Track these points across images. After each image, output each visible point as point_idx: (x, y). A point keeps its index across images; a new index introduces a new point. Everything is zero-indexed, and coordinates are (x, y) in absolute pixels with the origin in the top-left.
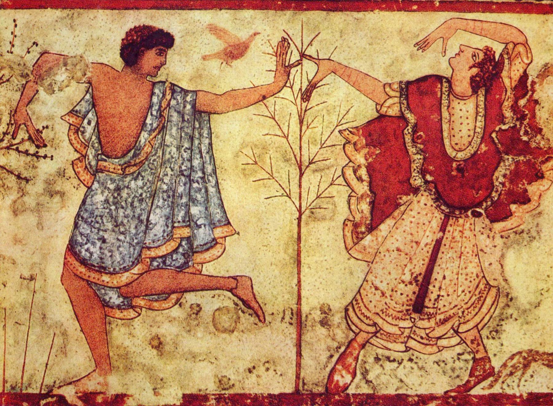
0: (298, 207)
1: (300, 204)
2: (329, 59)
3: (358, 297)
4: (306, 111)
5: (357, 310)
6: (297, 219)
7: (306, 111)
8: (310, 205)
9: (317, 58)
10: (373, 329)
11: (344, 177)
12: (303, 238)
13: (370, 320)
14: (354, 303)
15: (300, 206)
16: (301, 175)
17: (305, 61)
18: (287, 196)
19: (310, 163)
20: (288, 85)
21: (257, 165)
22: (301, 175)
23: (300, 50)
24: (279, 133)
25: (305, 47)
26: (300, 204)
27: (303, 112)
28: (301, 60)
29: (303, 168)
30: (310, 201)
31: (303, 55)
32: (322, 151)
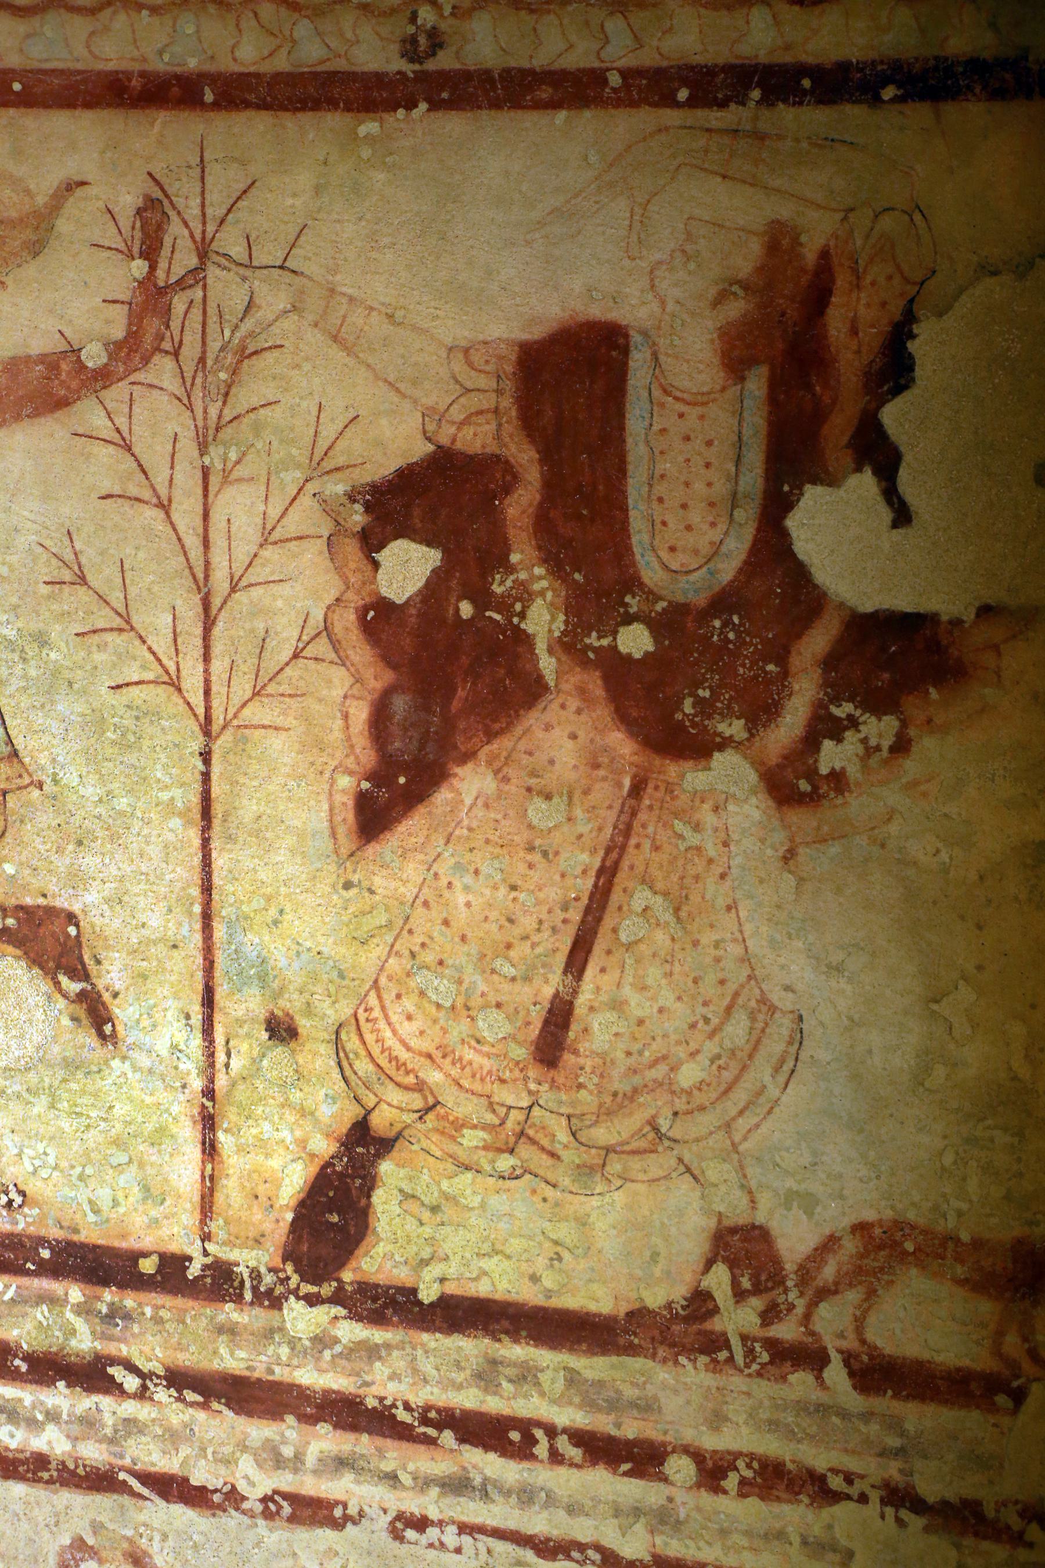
0: (202, 718)
1: (208, 709)
2: (281, 267)
3: (373, 1000)
4: (217, 429)
5: (370, 1038)
6: (201, 754)
7: (217, 429)
8: (235, 716)
9: (246, 261)
13: (408, 1073)
15: (208, 718)
16: (208, 624)
17: (213, 273)
18: (172, 684)
19: (233, 589)
20: (167, 345)
21: (82, 590)
22: (208, 624)
23: (198, 237)
24: (147, 494)
25: (211, 228)
26: (208, 709)
27: (211, 432)
29: (216, 602)
30: (236, 701)
31: (203, 252)
32: (267, 553)
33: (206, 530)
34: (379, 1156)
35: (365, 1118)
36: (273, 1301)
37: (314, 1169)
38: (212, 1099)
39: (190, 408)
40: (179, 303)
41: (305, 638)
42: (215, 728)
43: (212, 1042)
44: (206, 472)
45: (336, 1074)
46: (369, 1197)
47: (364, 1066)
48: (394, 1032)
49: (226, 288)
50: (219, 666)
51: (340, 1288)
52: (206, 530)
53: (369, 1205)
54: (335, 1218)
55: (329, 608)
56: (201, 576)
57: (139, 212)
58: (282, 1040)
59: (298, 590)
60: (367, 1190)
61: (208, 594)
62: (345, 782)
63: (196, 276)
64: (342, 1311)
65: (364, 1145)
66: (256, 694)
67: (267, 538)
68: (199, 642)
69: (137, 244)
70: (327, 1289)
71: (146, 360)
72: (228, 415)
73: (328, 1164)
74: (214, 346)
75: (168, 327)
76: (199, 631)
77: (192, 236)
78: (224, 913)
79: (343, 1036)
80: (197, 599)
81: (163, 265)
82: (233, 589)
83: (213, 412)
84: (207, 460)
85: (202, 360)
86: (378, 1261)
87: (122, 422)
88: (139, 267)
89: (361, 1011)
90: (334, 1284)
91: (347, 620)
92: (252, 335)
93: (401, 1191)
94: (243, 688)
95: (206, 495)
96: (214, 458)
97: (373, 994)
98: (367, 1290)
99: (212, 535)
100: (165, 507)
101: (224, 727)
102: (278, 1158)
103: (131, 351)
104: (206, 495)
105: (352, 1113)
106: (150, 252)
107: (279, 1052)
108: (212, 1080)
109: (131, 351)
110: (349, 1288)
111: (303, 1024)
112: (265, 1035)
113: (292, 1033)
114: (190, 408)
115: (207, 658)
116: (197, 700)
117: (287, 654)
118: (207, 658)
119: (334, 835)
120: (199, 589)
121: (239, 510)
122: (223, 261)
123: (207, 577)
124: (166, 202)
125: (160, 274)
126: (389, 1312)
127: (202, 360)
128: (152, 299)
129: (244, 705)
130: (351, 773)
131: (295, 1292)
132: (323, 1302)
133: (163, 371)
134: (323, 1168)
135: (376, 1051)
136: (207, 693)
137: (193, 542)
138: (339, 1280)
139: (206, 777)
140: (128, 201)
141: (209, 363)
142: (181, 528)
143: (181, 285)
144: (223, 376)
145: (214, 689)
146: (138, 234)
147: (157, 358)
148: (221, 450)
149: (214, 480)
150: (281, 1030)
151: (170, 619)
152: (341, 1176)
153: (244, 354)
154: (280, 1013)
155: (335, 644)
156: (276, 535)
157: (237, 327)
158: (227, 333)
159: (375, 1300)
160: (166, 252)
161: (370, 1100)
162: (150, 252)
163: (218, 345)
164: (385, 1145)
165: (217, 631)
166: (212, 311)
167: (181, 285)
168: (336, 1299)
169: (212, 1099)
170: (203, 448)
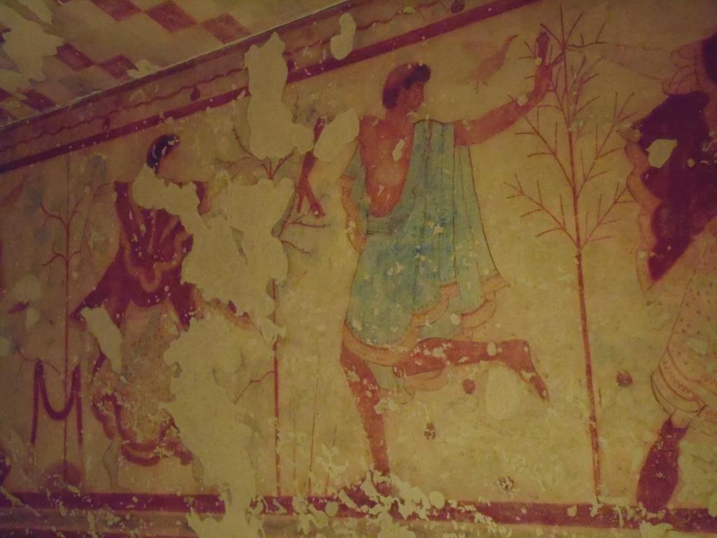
0: (576, 240)
2: (596, 43)
3: (667, 358)
4: (575, 115)
5: (668, 378)
6: (576, 257)
8: (590, 236)
10: (695, 407)
11: (629, 191)
12: (585, 280)
14: (662, 367)
15: (578, 239)
16: (576, 198)
17: (568, 54)
19: (585, 180)
20: (551, 88)
22: (576, 198)
25: (566, 37)
28: (563, 53)
29: (578, 188)
31: (564, 46)
33: (572, 158)
34: (679, 438)
35: (670, 420)
36: (634, 524)
37: (647, 451)
38: (595, 421)
39: (562, 110)
40: (555, 70)
41: (618, 194)
42: (582, 243)
43: (592, 392)
44: (570, 135)
45: (653, 399)
46: (676, 461)
47: (666, 392)
48: (680, 372)
49: (574, 58)
50: (581, 215)
51: (668, 514)
52: (572, 158)
53: (677, 466)
54: (660, 475)
55: (628, 178)
56: (570, 178)
57: (538, 40)
58: (625, 385)
59: (613, 173)
60: (675, 456)
61: (575, 186)
62: (643, 255)
63: (562, 57)
64: (669, 526)
65: (671, 432)
66: (599, 224)
67: (599, 154)
68: (572, 207)
69: (537, 52)
70: (661, 515)
71: (543, 96)
72: (578, 108)
73: (655, 446)
74: (570, 81)
75: (551, 80)
76: (571, 201)
77: (559, 42)
78: (592, 328)
79: (655, 378)
80: (569, 189)
81: (548, 57)
82: (585, 180)
83: (572, 108)
84: (570, 129)
85: (566, 89)
86: (686, 495)
87: (534, 123)
88: (538, 61)
89: (662, 364)
90: (664, 511)
91: (637, 182)
92: (586, 73)
93: (693, 456)
94: (593, 222)
95: (571, 144)
96: (573, 128)
97: (666, 354)
98: (681, 512)
99: (575, 161)
100: (554, 153)
101: (586, 243)
102: (630, 449)
103: (536, 95)
104: (571, 144)
105: (664, 417)
106: (542, 54)
107: (625, 391)
108: (594, 411)
109: (536, 95)
110: (672, 513)
111: (635, 376)
112: (617, 384)
113: (630, 381)
114: (562, 110)
115: (576, 212)
116: (573, 232)
117: (611, 202)
118: (576, 212)
119: (640, 281)
120: (571, 184)
121: (585, 146)
122: (571, 48)
123: (573, 178)
124: (548, 33)
125: (547, 62)
126: (695, 524)
127: (566, 89)
128: (545, 71)
129: (594, 230)
130: (645, 250)
131: (645, 518)
132: (660, 522)
133: (550, 99)
134: (652, 449)
135: (671, 384)
136: (577, 228)
137: (567, 165)
138: (667, 510)
139: (580, 267)
140: (532, 37)
141: (569, 89)
142: (561, 159)
143: (556, 62)
144: (575, 93)
145: (580, 226)
146: (537, 49)
147: (547, 95)
148: (576, 123)
149: (574, 139)
150: (624, 380)
151: (559, 199)
152: (662, 451)
153: (583, 82)
154: (623, 372)
155: (632, 193)
156: (602, 153)
157: (579, 72)
158: (575, 76)
159: (687, 517)
160: (549, 52)
161: (671, 409)
162: (542, 54)
163: (571, 82)
164: (681, 432)
165: (580, 200)
166: (568, 68)
167: (556, 62)
168: (667, 519)
169: (595, 421)
170: (568, 124)
